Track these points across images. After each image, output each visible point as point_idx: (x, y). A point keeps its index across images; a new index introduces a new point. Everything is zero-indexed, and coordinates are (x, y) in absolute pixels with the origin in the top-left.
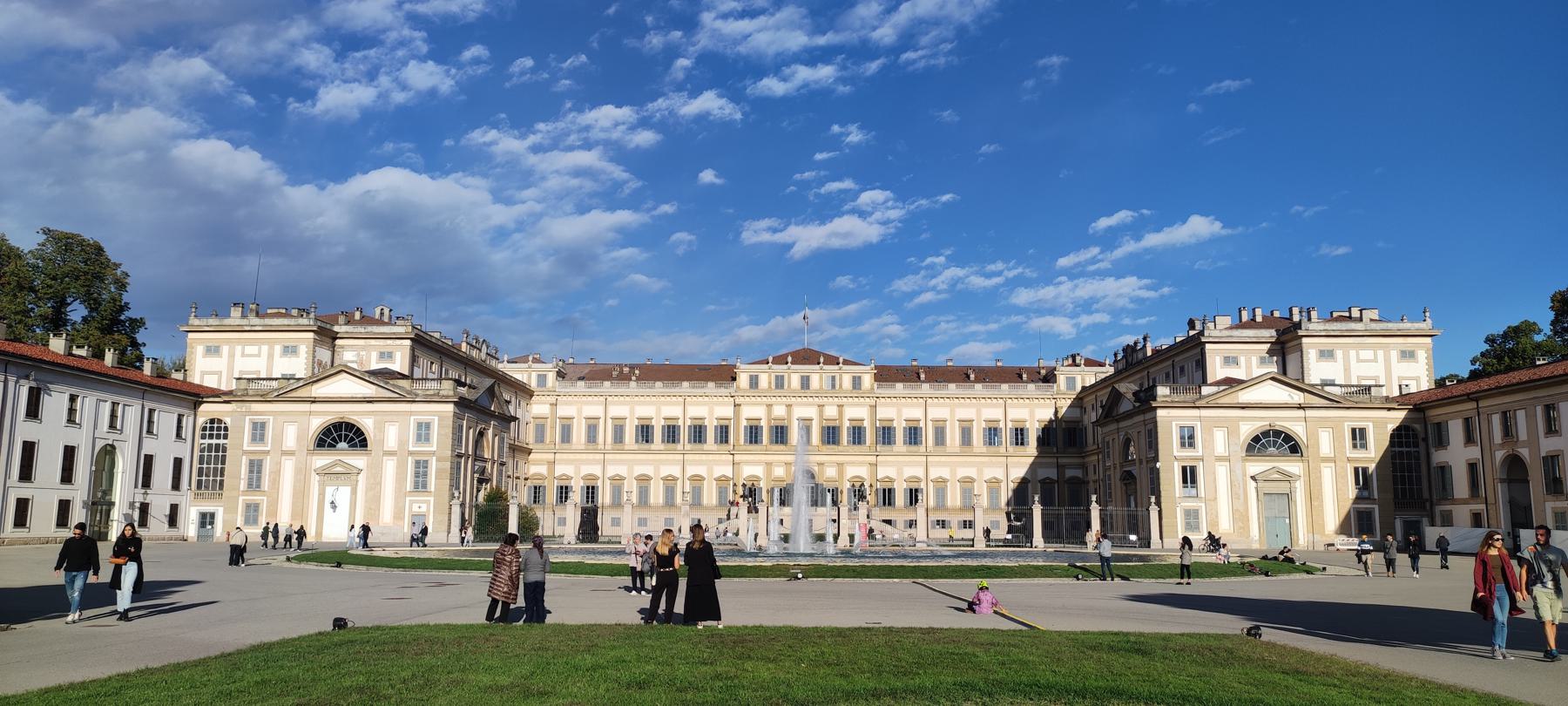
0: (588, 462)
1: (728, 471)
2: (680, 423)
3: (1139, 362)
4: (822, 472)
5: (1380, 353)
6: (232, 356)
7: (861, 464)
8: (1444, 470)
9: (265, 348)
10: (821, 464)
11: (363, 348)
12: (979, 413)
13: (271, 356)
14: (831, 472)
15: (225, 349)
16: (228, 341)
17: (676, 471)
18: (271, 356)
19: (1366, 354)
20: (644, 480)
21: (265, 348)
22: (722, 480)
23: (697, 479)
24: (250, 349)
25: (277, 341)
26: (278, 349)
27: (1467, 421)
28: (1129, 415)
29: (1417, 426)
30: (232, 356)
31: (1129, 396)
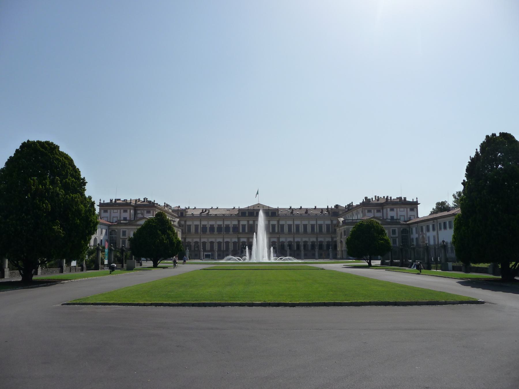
1: (236, 240)
3: (351, 209)
5: (405, 209)
6: (110, 213)
8: (413, 239)
9: (119, 211)
11: (142, 210)
12: (309, 222)
13: (120, 213)
15: (109, 211)
16: (110, 209)
17: (221, 240)
18: (120, 213)
19: (402, 209)
20: (212, 243)
21: (119, 211)
22: (235, 243)
23: (227, 243)
24: (115, 211)
25: (122, 209)
26: (122, 211)
27: (416, 229)
28: (341, 226)
29: (408, 229)
30: (110, 213)
31: (341, 222)
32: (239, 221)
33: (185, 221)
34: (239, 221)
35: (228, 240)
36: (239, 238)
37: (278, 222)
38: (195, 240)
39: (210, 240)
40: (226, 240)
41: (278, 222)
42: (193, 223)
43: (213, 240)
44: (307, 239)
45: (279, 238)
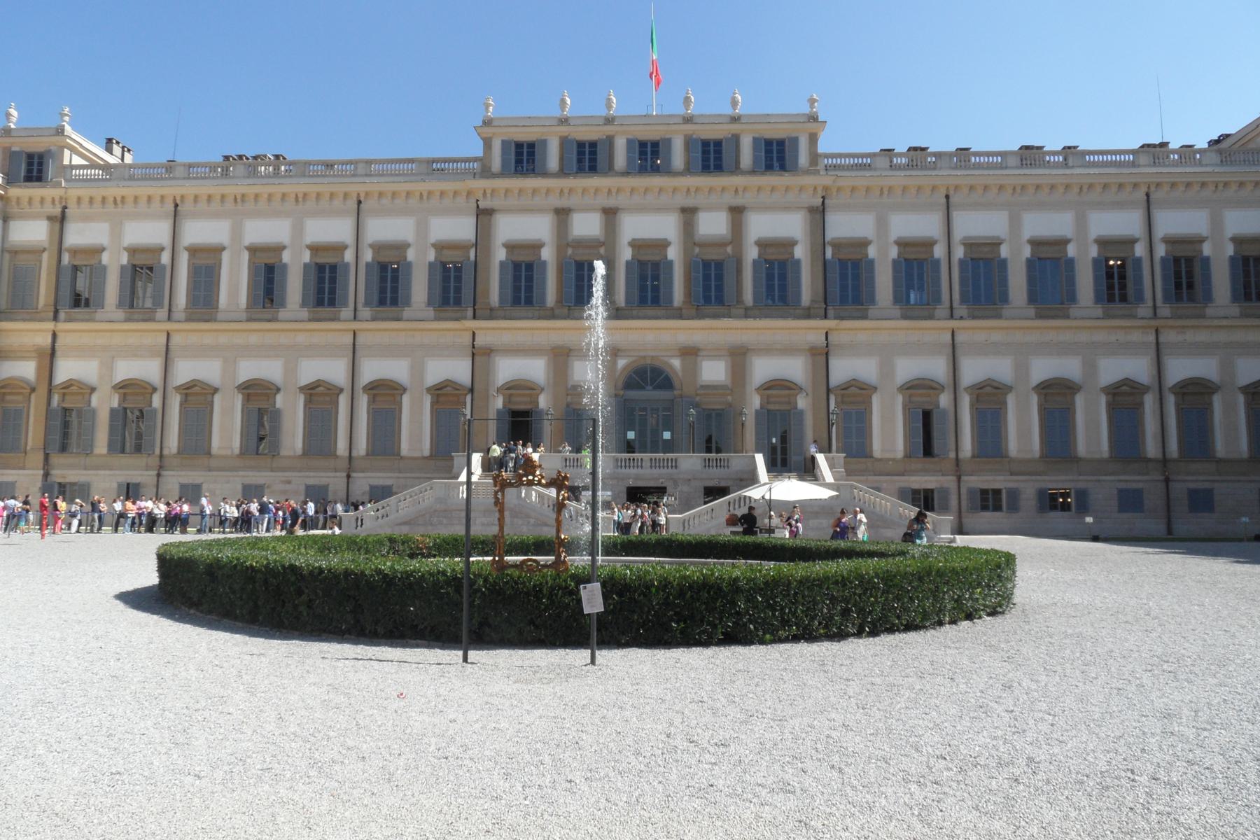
0: (134, 352)
1: (459, 370)
2: (349, 256)
4: (693, 371)
7: (788, 350)
10: (690, 353)
14: (714, 372)
17: (334, 371)
22: (444, 394)
23: (385, 394)
32: (484, 215)
33: (60, 220)
34: (484, 215)
35: (395, 369)
36: (479, 355)
37: (818, 214)
38: (126, 370)
39: (249, 370)
40: (371, 370)
41: (818, 214)
42: (116, 233)
43: (269, 369)
44: (1069, 368)
45: (822, 355)
